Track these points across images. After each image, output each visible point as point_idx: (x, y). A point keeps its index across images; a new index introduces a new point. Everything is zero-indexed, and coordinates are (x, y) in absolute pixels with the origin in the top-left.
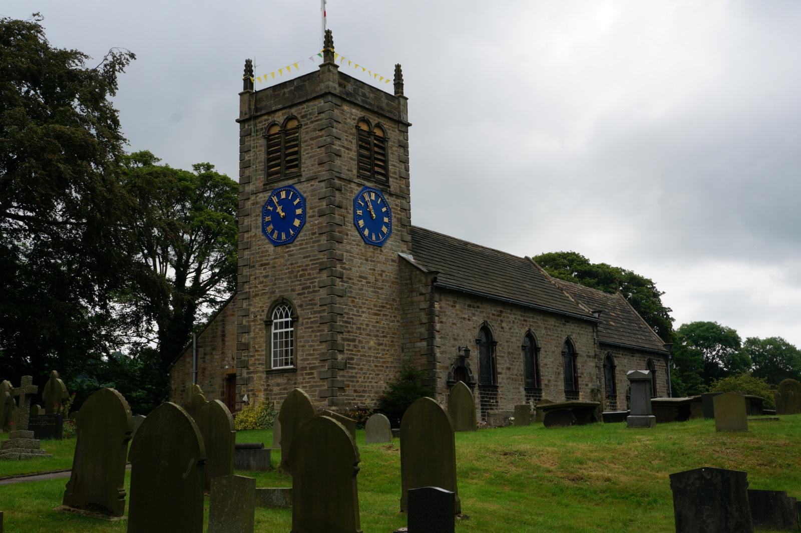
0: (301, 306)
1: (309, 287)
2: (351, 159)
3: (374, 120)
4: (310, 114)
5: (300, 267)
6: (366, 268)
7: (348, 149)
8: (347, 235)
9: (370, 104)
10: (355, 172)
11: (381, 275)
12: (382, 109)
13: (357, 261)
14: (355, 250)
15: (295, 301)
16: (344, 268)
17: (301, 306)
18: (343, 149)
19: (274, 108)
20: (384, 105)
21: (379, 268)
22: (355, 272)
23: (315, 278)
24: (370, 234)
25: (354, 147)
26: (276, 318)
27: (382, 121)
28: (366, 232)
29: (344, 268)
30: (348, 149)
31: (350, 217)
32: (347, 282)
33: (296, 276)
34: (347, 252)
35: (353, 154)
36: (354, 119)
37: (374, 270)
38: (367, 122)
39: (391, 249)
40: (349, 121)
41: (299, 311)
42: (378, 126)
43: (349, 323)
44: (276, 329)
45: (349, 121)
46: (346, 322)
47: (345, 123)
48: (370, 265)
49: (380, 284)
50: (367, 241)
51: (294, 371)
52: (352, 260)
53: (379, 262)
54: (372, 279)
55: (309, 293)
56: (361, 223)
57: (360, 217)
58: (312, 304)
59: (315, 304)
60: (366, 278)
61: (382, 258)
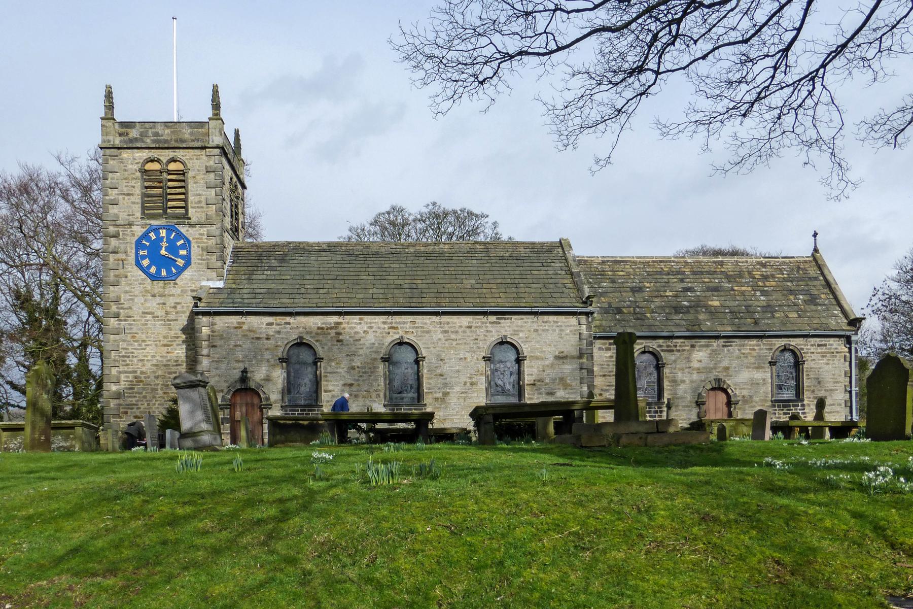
2: (133, 203)
3: (165, 155)
6: (153, 304)
7: (128, 195)
8: (126, 277)
9: (166, 141)
10: (139, 214)
11: (175, 307)
12: (182, 141)
13: (139, 300)
14: (137, 289)
16: (122, 308)
18: (121, 197)
20: (186, 136)
21: (171, 301)
22: (137, 311)
24: (158, 271)
25: (138, 191)
27: (179, 154)
28: (153, 270)
30: (128, 195)
31: (132, 259)
32: (125, 320)
34: (126, 292)
35: (138, 199)
36: (137, 163)
37: (164, 304)
38: (158, 161)
39: (192, 279)
40: (130, 166)
42: (173, 160)
43: (129, 357)
45: (130, 166)
46: (123, 356)
47: (125, 170)
48: (159, 300)
49: (172, 317)
50: (154, 278)
52: (133, 300)
53: (173, 295)
54: (160, 313)
56: (146, 262)
57: (143, 257)
60: (152, 313)
61: (177, 291)
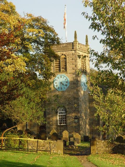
0: (68, 108)
1: (71, 103)
4: (70, 55)
5: (68, 97)
15: (66, 107)
17: (68, 108)
19: (58, 51)
23: (73, 101)
26: (59, 111)
29: (80, 98)
33: (67, 100)
41: (67, 110)
44: (59, 113)
51: (66, 126)
55: (71, 105)
58: (72, 108)
59: (73, 108)
